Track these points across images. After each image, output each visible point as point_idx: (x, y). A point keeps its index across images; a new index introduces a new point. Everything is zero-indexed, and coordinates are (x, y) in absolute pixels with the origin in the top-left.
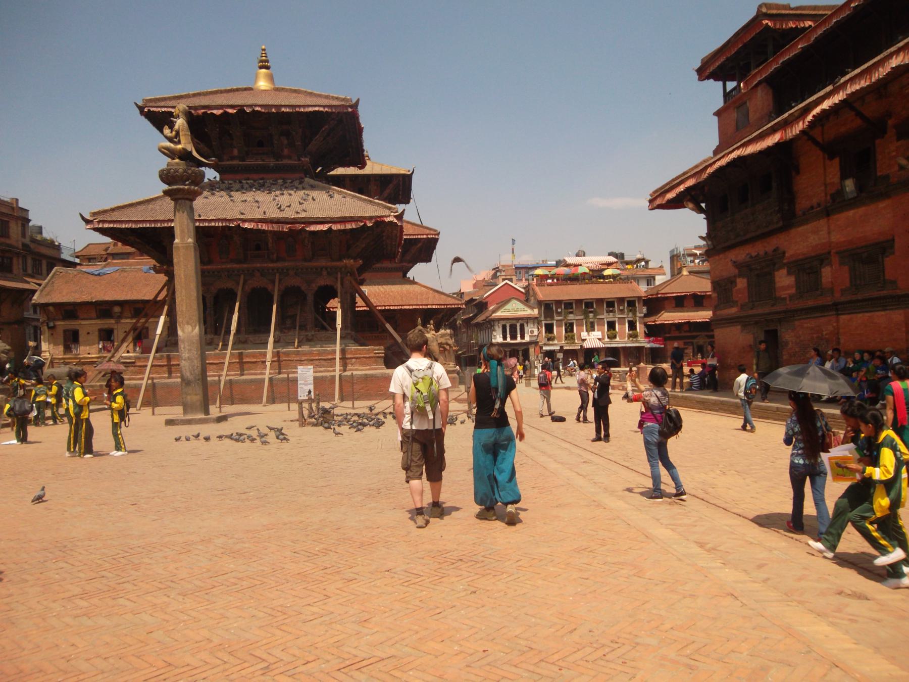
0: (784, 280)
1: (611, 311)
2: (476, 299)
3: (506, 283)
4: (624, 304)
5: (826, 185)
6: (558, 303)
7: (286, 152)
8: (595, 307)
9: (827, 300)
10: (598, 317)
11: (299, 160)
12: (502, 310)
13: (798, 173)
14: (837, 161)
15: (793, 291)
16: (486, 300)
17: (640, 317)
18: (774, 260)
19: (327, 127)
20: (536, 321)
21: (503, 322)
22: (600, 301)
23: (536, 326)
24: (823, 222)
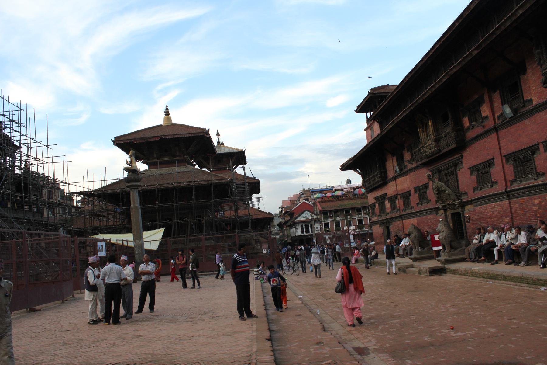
0: (388, 205)
1: (360, 214)
3: (304, 202)
6: (331, 211)
7: (178, 154)
9: (398, 214)
10: (353, 217)
11: (184, 157)
12: (300, 217)
13: (386, 161)
15: (390, 210)
19: (195, 141)
20: (319, 222)
21: (301, 224)
22: (353, 209)
23: (319, 224)
24: (394, 181)
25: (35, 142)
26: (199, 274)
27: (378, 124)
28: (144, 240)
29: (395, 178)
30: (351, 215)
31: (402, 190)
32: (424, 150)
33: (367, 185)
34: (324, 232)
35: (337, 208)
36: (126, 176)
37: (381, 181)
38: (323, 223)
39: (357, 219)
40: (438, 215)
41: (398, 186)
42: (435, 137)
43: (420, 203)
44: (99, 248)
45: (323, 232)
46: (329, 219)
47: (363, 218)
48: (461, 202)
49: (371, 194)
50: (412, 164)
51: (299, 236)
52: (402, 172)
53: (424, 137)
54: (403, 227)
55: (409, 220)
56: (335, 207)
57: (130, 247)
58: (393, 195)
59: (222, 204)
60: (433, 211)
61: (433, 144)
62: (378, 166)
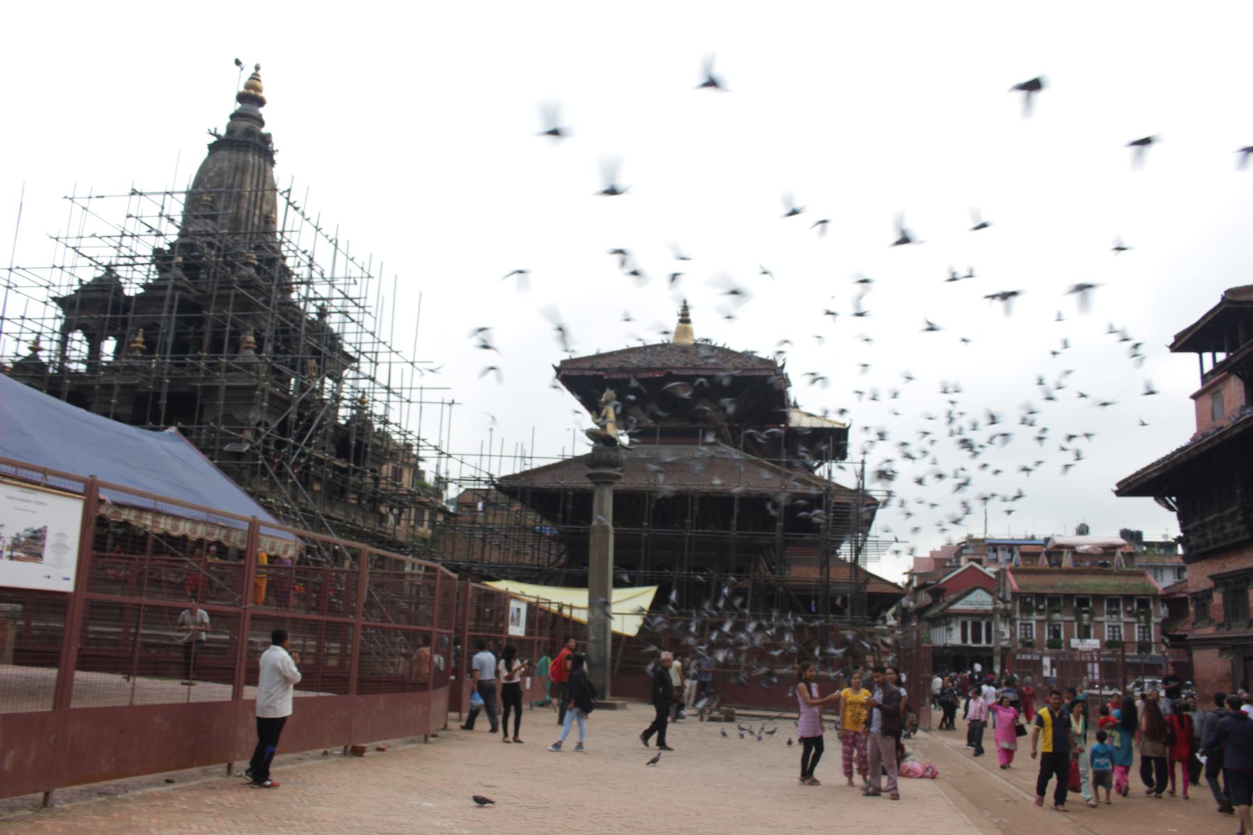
1: (1115, 613)
2: (931, 585)
3: (972, 567)
4: (1133, 603)
6: (1040, 597)
8: (1091, 604)
12: (962, 601)
17: (1156, 624)
20: (1008, 621)
21: (964, 619)
22: (1098, 598)
23: (1008, 625)
25: (389, 350)
26: (738, 712)
27: (1242, 383)
28: (614, 609)
30: (1092, 614)
33: (1193, 541)
34: (1019, 646)
35: (1058, 591)
36: (588, 450)
37: (1244, 534)
38: (1018, 622)
39: (1106, 625)
44: (513, 617)
45: (1016, 646)
46: (1035, 616)
47: (1122, 624)
49: (1199, 564)
51: (954, 648)
56: (1052, 587)
57: (577, 624)
59: (789, 548)
62: (1238, 491)
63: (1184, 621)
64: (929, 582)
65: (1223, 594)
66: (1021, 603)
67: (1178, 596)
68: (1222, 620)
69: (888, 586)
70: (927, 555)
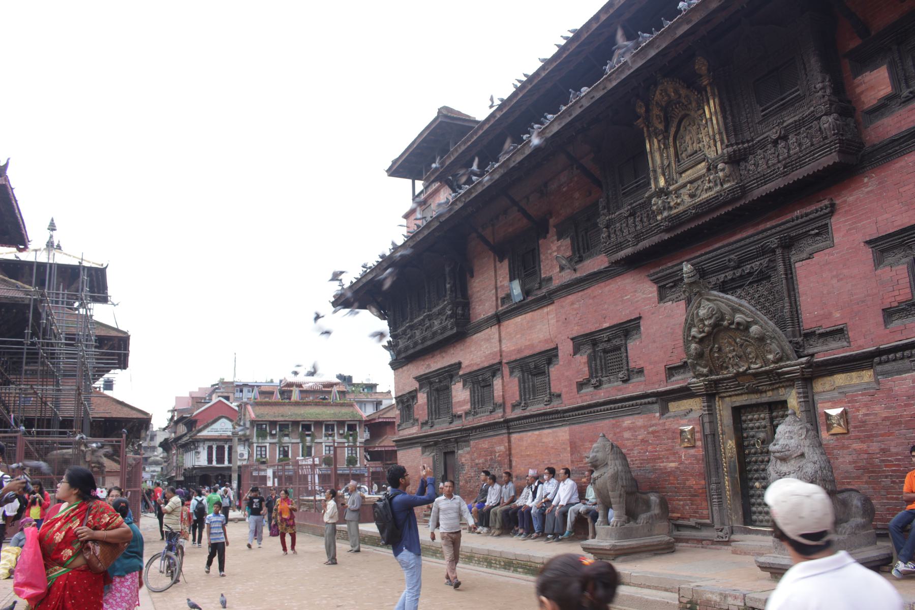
0: (460, 394)
1: (330, 435)
2: (187, 417)
3: (220, 401)
4: (344, 427)
5: (496, 288)
6: (273, 424)
8: (313, 429)
9: (498, 416)
10: (317, 440)
12: (209, 429)
13: (472, 276)
14: (506, 263)
15: (468, 407)
16: (196, 418)
18: (451, 372)
20: (247, 444)
21: (210, 444)
22: (318, 424)
23: (247, 448)
24: (495, 329)
29: (498, 319)
31: (519, 351)
32: (664, 202)
33: (402, 344)
35: (287, 419)
37: (452, 329)
38: (255, 445)
40: (667, 415)
41: (504, 341)
42: (727, 146)
43: (593, 381)
46: (269, 439)
48: (810, 364)
49: (405, 368)
50: (575, 270)
51: (201, 468)
52: (530, 298)
53: (666, 163)
54: (510, 454)
55: (537, 432)
56: (282, 416)
58: (486, 364)
60: (649, 403)
61: (723, 170)
62: (448, 286)
63: (381, 440)
64: (184, 416)
65: (428, 393)
66: (257, 429)
67: (377, 421)
68: (426, 418)
69: (134, 412)
70: (188, 395)
